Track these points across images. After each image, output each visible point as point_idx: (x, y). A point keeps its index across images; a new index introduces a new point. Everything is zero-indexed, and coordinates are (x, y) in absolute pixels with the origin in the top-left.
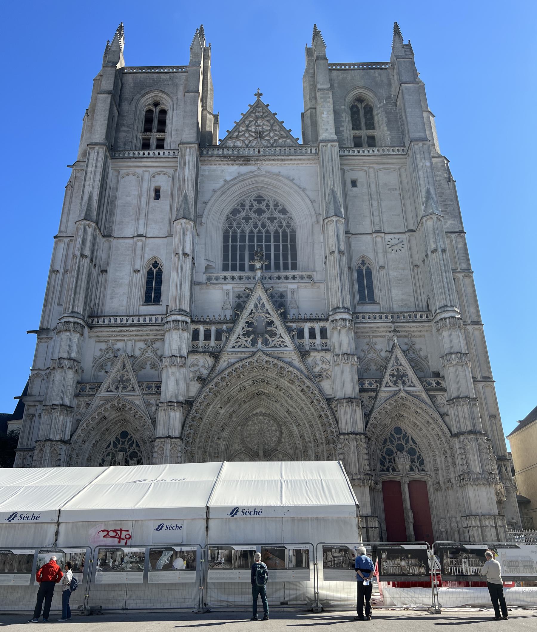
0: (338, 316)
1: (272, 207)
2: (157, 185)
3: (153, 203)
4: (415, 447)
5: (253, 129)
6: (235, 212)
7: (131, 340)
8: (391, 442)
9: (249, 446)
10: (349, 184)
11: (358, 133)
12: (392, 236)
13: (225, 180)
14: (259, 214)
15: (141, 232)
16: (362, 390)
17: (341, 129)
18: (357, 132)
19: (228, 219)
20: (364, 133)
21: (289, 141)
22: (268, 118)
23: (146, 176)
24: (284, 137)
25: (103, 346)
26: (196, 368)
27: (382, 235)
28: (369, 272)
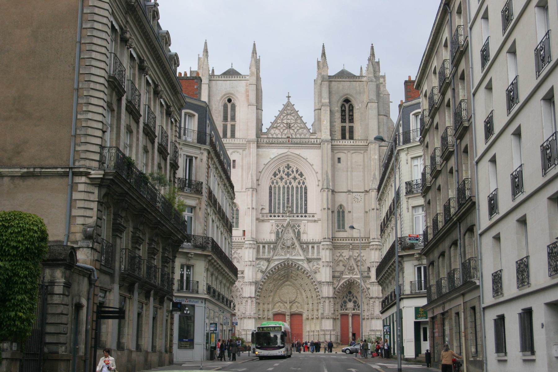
6: (275, 175)
8: (346, 298)
9: (283, 299)
11: (344, 124)
14: (288, 177)
16: (334, 277)
20: (347, 125)
21: (305, 130)
22: (293, 115)
26: (259, 266)
28: (343, 212)
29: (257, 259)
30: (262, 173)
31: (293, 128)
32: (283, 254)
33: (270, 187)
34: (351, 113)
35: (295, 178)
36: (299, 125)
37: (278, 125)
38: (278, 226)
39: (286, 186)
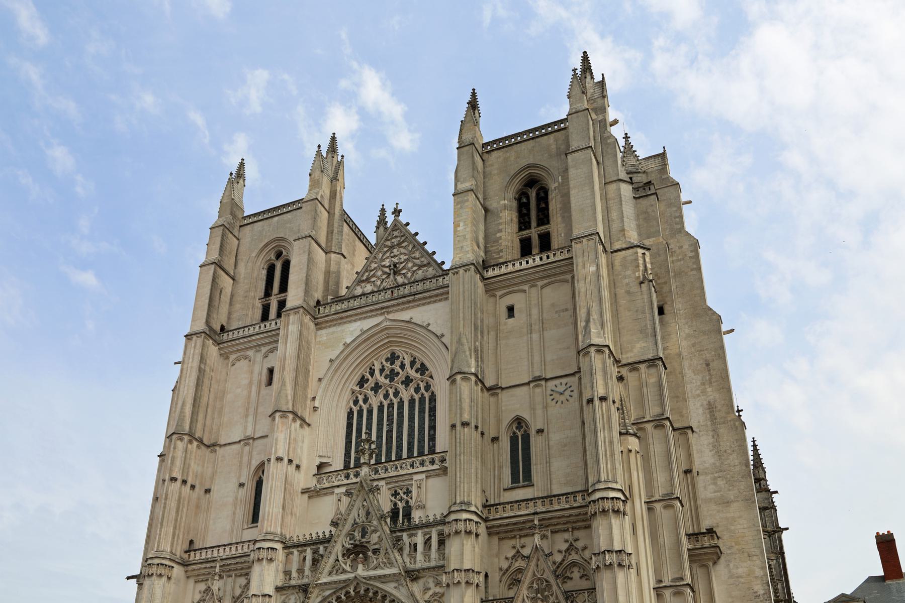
0: (453, 517)
1: (408, 366)
2: (270, 366)
3: (265, 391)
6: (362, 382)
7: (231, 576)
10: (504, 312)
12: (557, 382)
14: (392, 380)
15: (249, 432)
17: (498, 235)
21: (430, 269)
23: (259, 356)
24: (425, 265)
25: (202, 587)
27: (543, 383)
28: (526, 438)
30: (324, 382)
32: (348, 568)
33: (350, 414)
35: (407, 381)
36: (417, 262)
39: (386, 403)
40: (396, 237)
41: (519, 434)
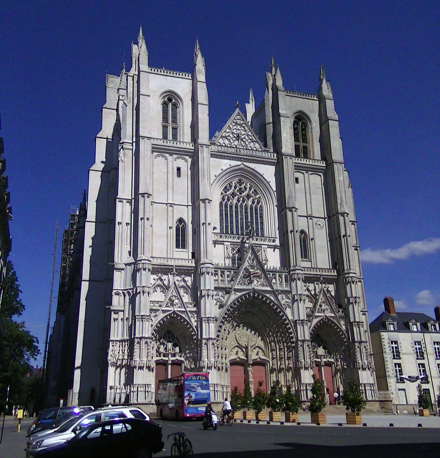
2: (179, 166)
4: (326, 346)
5: (235, 131)
9: (240, 343)
12: (318, 219)
13: (222, 170)
14: (241, 194)
18: (297, 143)
19: (221, 194)
24: (255, 141)
26: (218, 297)
27: (313, 218)
29: (216, 289)
30: (214, 185)
31: (244, 140)
34: (304, 133)
36: (251, 137)
37: (227, 134)
38: (233, 249)
40: (238, 119)
41: (302, 237)
